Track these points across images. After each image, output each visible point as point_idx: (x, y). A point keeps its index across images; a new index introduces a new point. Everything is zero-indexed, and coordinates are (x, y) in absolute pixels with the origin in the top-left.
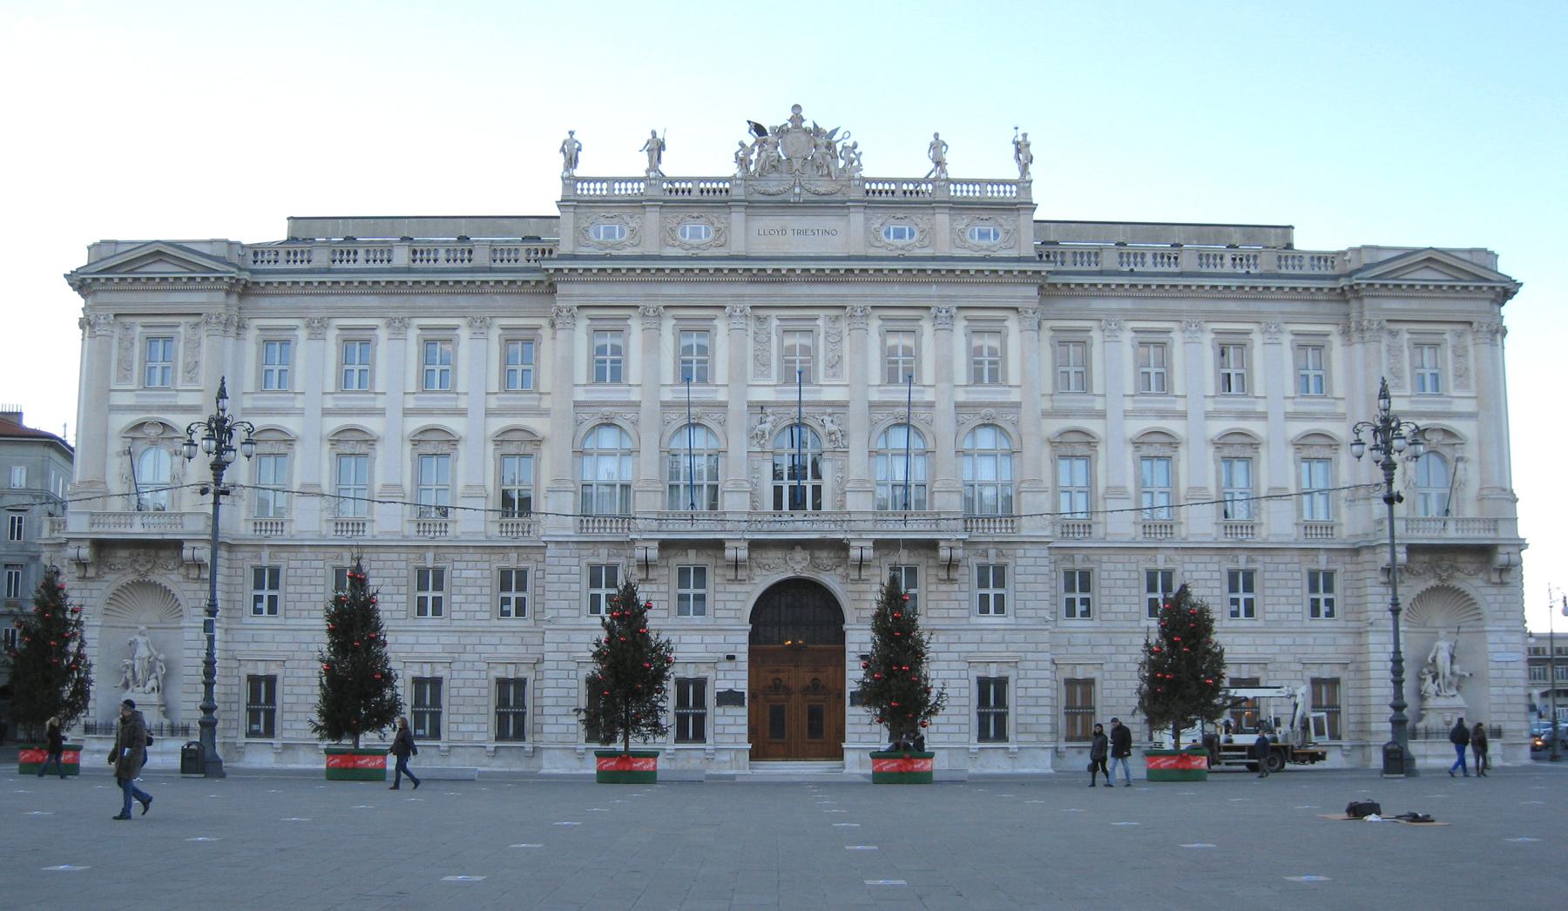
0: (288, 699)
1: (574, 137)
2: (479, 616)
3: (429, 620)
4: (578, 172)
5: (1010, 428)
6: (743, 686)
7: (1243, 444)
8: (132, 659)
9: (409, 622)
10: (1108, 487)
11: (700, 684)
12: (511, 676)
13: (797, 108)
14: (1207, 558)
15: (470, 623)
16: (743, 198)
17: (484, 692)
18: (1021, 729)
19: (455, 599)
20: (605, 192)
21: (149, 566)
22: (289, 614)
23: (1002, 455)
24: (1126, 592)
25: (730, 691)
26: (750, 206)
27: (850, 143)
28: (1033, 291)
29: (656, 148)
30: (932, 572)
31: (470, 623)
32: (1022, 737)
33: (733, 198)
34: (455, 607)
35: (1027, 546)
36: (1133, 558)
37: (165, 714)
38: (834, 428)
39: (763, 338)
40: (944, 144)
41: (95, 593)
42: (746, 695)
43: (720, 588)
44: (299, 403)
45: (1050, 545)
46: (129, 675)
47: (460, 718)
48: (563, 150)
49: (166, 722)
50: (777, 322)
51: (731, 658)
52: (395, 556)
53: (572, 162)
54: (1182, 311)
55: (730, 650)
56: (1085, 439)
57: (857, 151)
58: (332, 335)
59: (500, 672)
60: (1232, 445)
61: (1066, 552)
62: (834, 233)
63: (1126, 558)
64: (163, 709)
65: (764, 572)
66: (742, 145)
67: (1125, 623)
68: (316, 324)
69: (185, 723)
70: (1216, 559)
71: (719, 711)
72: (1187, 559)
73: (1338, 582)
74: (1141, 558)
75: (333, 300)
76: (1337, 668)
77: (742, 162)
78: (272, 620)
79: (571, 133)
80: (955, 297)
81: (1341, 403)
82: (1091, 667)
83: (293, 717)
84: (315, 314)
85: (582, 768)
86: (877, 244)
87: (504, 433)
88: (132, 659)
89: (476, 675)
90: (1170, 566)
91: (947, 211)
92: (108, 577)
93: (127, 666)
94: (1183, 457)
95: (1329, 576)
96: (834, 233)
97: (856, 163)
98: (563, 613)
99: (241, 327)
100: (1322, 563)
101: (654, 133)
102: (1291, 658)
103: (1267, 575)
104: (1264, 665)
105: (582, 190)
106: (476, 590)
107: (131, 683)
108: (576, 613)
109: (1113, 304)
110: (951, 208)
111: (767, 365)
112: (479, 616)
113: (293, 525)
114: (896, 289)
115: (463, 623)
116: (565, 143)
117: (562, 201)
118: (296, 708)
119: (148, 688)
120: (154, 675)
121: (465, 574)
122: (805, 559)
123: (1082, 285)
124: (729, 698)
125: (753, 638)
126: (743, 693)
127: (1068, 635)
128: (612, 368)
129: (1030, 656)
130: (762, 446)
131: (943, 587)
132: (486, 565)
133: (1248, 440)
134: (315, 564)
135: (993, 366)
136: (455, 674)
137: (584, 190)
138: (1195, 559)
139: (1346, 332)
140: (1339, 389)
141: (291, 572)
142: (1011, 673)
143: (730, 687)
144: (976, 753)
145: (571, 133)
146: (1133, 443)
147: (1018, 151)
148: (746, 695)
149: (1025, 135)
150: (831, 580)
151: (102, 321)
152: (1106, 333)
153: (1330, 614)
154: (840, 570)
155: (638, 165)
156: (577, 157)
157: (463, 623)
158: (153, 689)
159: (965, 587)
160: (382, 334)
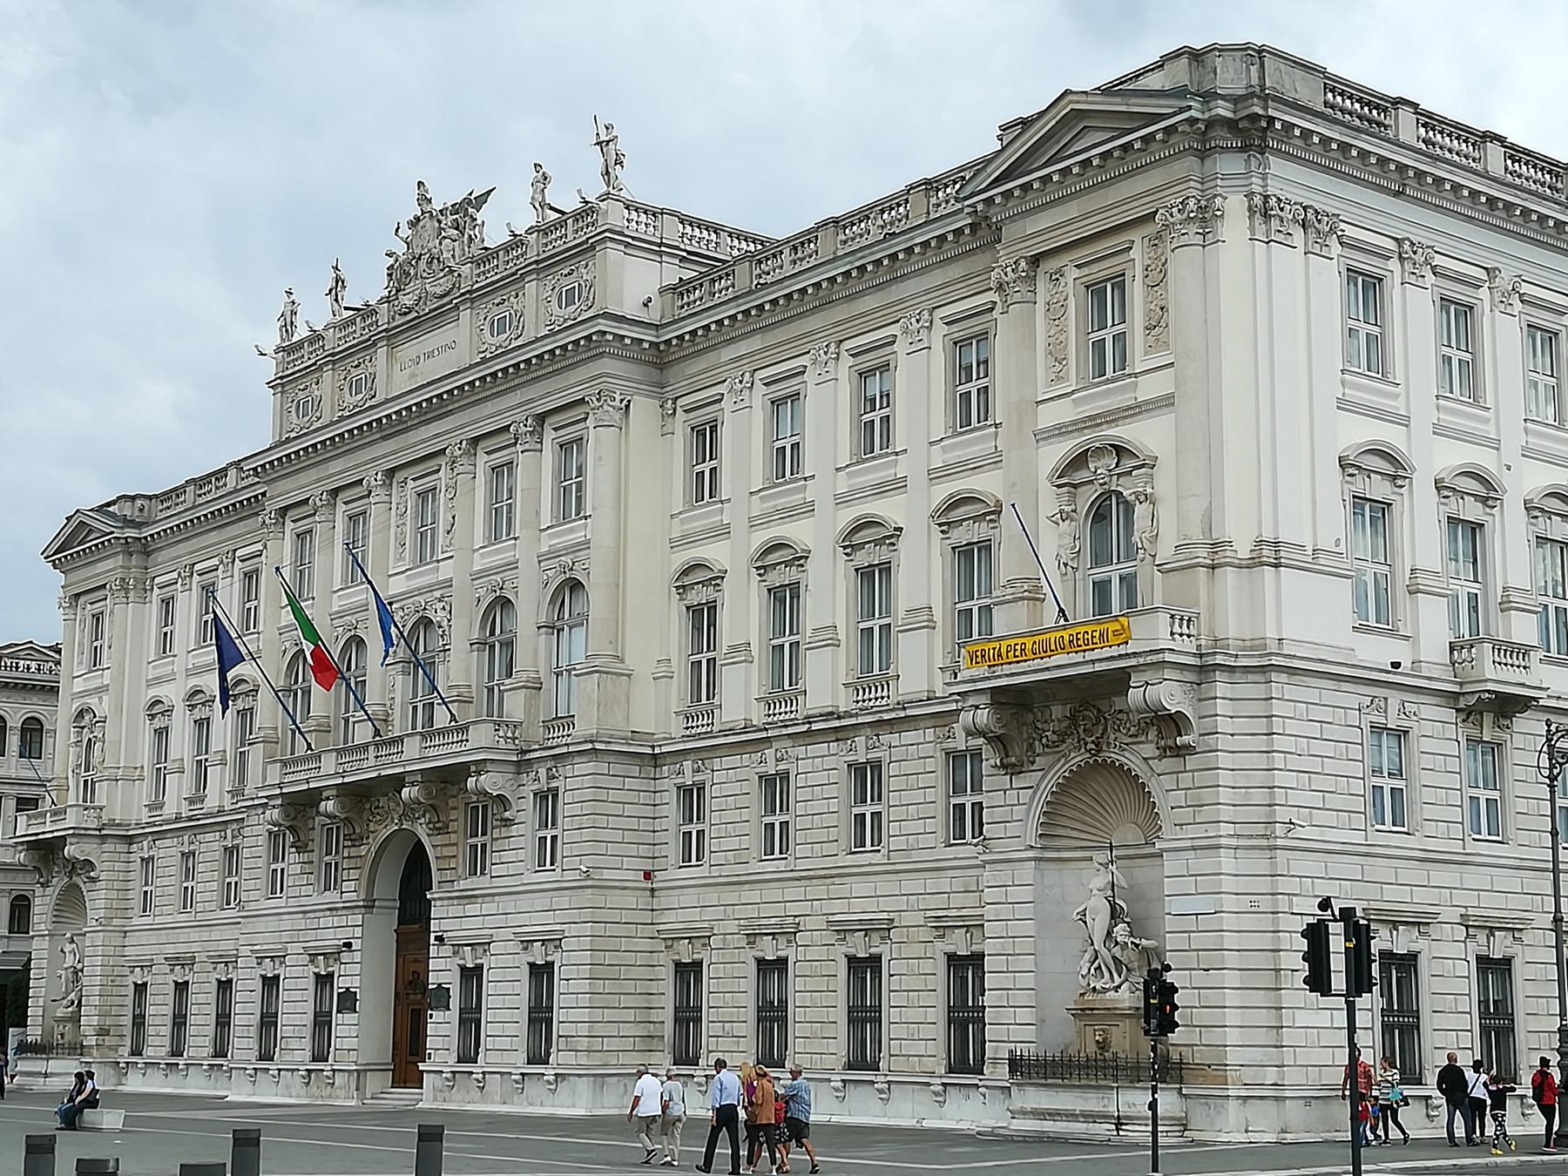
13: (420, 184)
51: (348, 945)
54: (811, 333)
63: (735, 760)
65: (377, 827)
85: (254, 1094)
109: (742, 348)
110: (538, 271)
124: (348, 1001)
138: (813, 750)
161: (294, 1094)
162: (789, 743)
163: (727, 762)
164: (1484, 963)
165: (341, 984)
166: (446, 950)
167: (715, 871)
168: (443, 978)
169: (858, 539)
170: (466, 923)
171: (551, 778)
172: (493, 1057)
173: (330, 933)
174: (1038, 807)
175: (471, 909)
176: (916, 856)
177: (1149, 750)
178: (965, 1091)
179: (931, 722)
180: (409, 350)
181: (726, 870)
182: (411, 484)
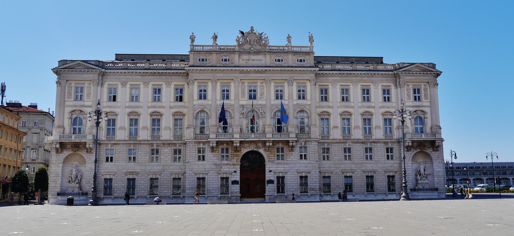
0: (115, 185)
1: (193, 34)
2: (168, 161)
4: (194, 44)
5: (308, 111)
6: (238, 179)
7: (369, 115)
9: (150, 163)
10: (376, 126)
11: (227, 178)
13: (252, 27)
14: (359, 144)
16: (238, 51)
17: (170, 182)
18: (311, 189)
19: (162, 157)
20: (202, 49)
21: (76, 149)
22: (116, 162)
23: (325, 119)
24: (338, 153)
25: (235, 180)
26: (240, 53)
27: (266, 37)
28: (314, 75)
29: (215, 38)
30: (288, 149)
32: (311, 192)
33: (236, 51)
34: (162, 159)
36: (340, 145)
37: (81, 190)
38: (262, 111)
39: (243, 88)
40: (291, 37)
41: (61, 157)
42: (239, 181)
43: (232, 154)
44: (119, 104)
45: (318, 141)
47: (163, 189)
48: (190, 38)
49: (81, 192)
50: (247, 84)
51: (235, 172)
52: (145, 146)
53: (193, 41)
55: (235, 170)
56: (327, 114)
57: (268, 39)
58: (128, 86)
59: (174, 176)
60: (366, 115)
61: (323, 143)
62: (262, 60)
63: (338, 145)
64: (80, 188)
65: (244, 149)
66: (238, 37)
67: (338, 162)
68: (124, 84)
69: (87, 192)
70: (362, 144)
71: (232, 186)
72: (354, 145)
73: (394, 151)
74: (342, 144)
75: (128, 77)
76: (394, 173)
77: (238, 41)
78: (111, 163)
79: (193, 33)
80: (294, 77)
81: (394, 104)
82: (329, 173)
83: (117, 190)
84: (123, 80)
86: (273, 63)
87: (364, 112)
88: (71, 175)
89: (167, 177)
90: (350, 146)
91: (291, 54)
92: (64, 152)
93: (70, 177)
94: (353, 118)
95: (392, 149)
96: (262, 60)
97: (268, 42)
98: (190, 160)
99: (102, 85)
100: (390, 145)
101: (215, 34)
102: (382, 170)
103: (375, 149)
104: (375, 172)
105: (195, 48)
106: (168, 155)
107: (71, 181)
108: (194, 160)
109: (335, 78)
111: (244, 95)
112: (168, 161)
113: (140, 137)
114: (278, 75)
116: (191, 36)
117: (190, 51)
118: (118, 187)
119: (76, 183)
120: (77, 179)
121: (164, 150)
122: (254, 145)
123: (326, 74)
124: (234, 182)
125: (241, 166)
126: (238, 181)
127: (323, 165)
128: (204, 96)
129: (314, 170)
130: (243, 116)
131: (290, 153)
132: (170, 148)
133: (370, 114)
134: (123, 148)
135: (303, 95)
136: (162, 177)
137: (196, 48)
138: (356, 145)
139: (396, 86)
141: (117, 150)
142: (309, 175)
144: (299, 196)
145: (193, 33)
146: (340, 115)
147: (310, 39)
148: (239, 181)
149: (312, 35)
150: (261, 151)
151: (63, 82)
152: (375, 86)
153: (392, 159)
154: (264, 148)
155: (211, 42)
156: (194, 40)
158: (77, 183)
159: (296, 153)
160: (142, 86)
162: (351, 143)
163: (335, 145)
165: (232, 178)
167: (333, 162)
168: (272, 179)
169: (365, 113)
170: (278, 169)
171: (305, 144)
172: (289, 192)
173: (155, 168)
174: (412, 156)
175: (279, 166)
176: (380, 161)
177: (431, 150)
178: (392, 194)
179: (383, 143)
180: (245, 57)
181: (336, 162)
182: (246, 84)
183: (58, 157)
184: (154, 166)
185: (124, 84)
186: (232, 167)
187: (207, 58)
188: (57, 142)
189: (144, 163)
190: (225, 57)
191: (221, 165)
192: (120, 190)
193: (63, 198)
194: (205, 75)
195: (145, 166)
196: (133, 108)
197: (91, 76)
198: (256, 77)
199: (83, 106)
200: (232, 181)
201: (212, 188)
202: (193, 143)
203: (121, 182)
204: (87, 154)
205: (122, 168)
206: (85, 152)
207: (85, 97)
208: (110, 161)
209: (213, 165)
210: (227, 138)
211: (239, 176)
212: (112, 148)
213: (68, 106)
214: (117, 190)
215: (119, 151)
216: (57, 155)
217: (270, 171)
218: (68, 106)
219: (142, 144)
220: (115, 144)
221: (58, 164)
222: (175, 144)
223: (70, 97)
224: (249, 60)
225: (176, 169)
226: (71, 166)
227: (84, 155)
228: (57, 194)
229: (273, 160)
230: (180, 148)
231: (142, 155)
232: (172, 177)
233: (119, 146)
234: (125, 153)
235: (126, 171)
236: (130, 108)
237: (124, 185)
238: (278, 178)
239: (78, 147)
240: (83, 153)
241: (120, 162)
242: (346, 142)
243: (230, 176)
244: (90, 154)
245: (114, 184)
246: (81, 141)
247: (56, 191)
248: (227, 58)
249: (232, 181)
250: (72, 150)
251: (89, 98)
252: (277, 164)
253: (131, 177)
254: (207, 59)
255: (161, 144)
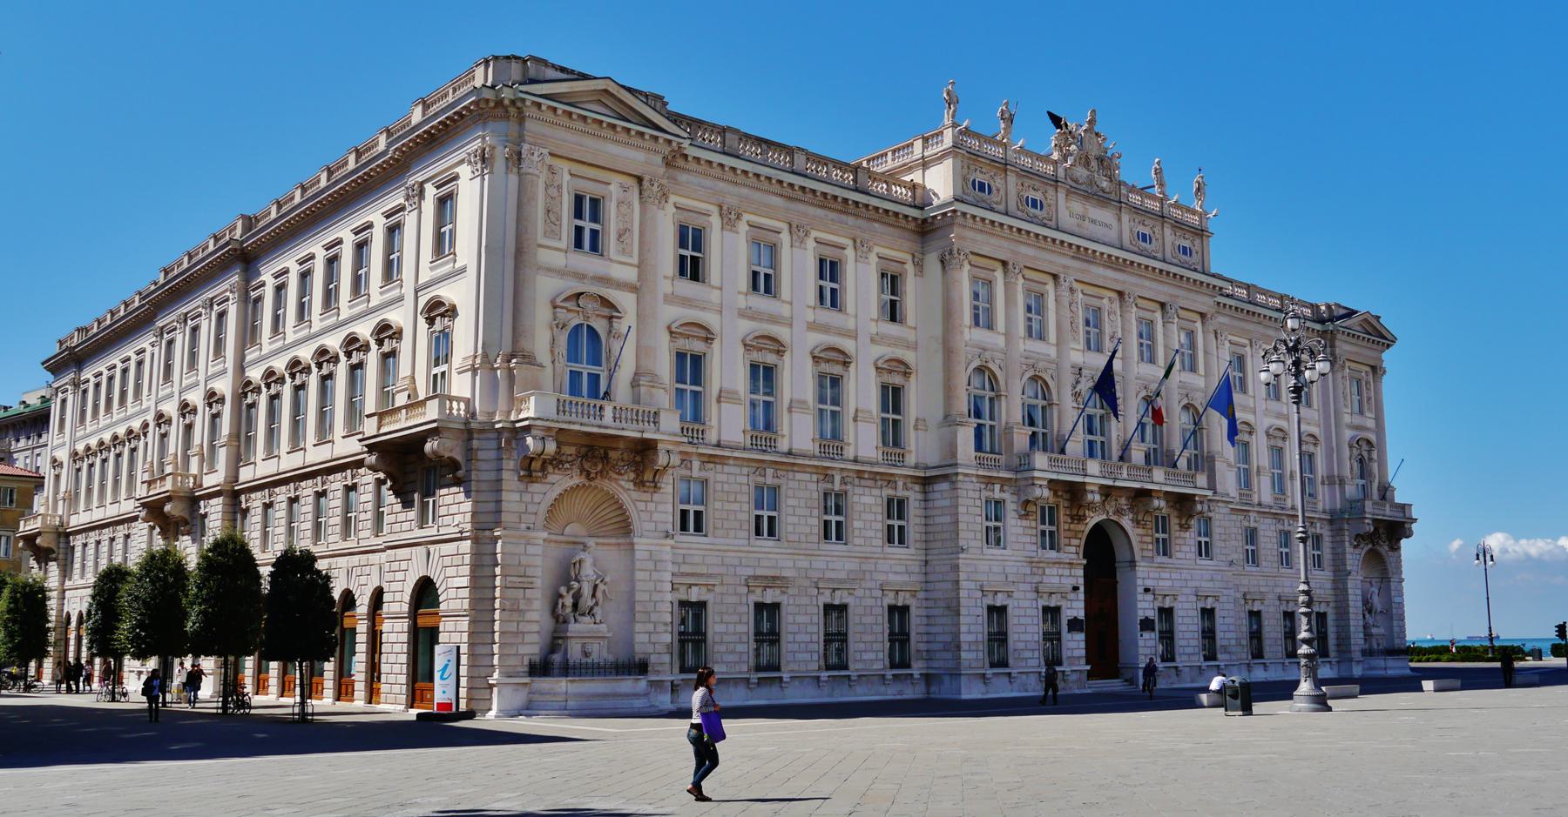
3: (834, 547)
6: (1081, 615)
8: (579, 582)
12: (900, 604)
15: (869, 549)
25: (1075, 617)
30: (1177, 521)
31: (869, 549)
35: (1219, 504)
46: (569, 601)
52: (806, 477)
58: (743, 227)
65: (1092, 514)
71: (1069, 636)
83: (723, 648)
85: (987, 692)
92: (551, 478)
115: (863, 549)
124: (1074, 625)
131: (1182, 534)
132: (876, 492)
140: (1315, 406)
143: (1076, 615)
150: (1126, 522)
151: (535, 158)
157: (863, 549)
161: (1030, 688)
164: (1251, 613)
166: (1149, 597)
183: (527, 498)
184: (835, 559)
185: (730, 217)
186: (1067, 572)
187: (992, 184)
188: (549, 429)
189: (804, 545)
190: (1032, 192)
191: (1041, 565)
192: (733, 652)
193: (575, 685)
194: (993, 240)
195: (807, 555)
196: (761, 320)
197: (640, 156)
198: (1105, 278)
199: (605, 280)
200: (1069, 620)
201: (1024, 644)
202: (974, 479)
203: (735, 618)
204: (635, 495)
205: (736, 562)
206: (631, 485)
207: (611, 243)
208: (695, 531)
209: (1025, 564)
210: (1071, 472)
211: (1082, 605)
212: (704, 474)
213: (550, 270)
214: (723, 648)
215: (726, 487)
216: (522, 486)
217: (1147, 590)
218: (550, 270)
219: (795, 469)
220: (711, 459)
221: (528, 528)
222: (890, 480)
223: (552, 233)
224: (1083, 218)
225: (896, 573)
226: (556, 542)
227: (625, 498)
228: (526, 669)
229: (1150, 554)
230: (906, 494)
231: (798, 511)
232: (753, 598)
233: (726, 469)
234: (746, 499)
235: (750, 572)
236: (752, 318)
237: (742, 628)
238: (1161, 610)
239: (605, 457)
240: (623, 487)
241: (732, 533)
242: (1249, 511)
243: (1063, 604)
244: (649, 495)
245: (715, 627)
246: (646, 435)
247: (523, 655)
248: (1038, 196)
249: (1069, 620)
250: (582, 470)
251: (624, 249)
252: (1159, 570)
253: (770, 597)
254: (994, 189)
255: (851, 474)
